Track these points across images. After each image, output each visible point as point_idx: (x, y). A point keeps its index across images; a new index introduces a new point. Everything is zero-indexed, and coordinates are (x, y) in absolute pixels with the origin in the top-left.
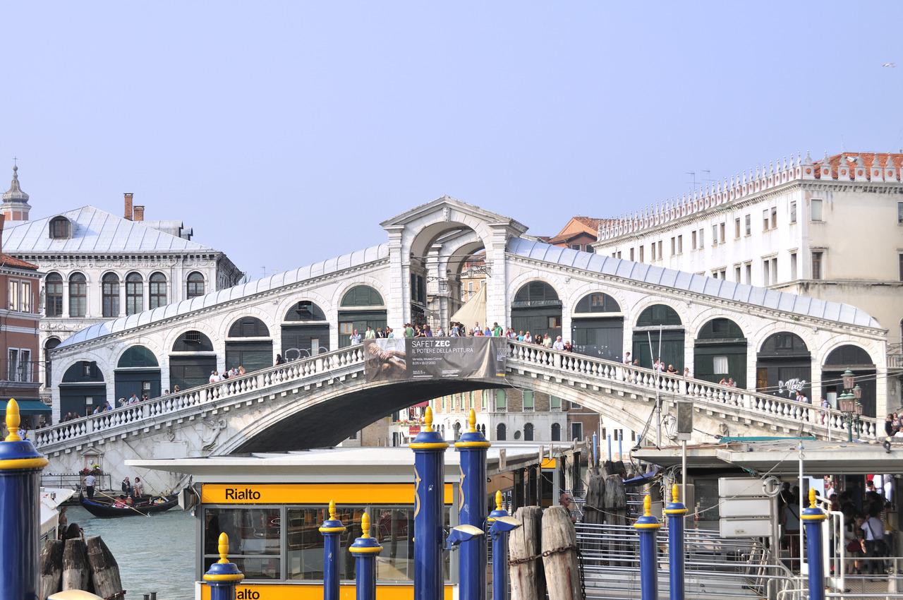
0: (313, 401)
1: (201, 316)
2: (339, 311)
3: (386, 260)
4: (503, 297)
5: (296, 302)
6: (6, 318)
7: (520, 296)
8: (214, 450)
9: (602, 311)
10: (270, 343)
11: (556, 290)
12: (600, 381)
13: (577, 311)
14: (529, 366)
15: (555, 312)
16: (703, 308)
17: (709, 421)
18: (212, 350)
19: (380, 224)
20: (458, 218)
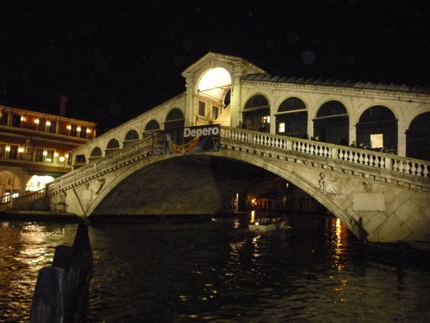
5: (149, 121)
7: (248, 105)
13: (279, 111)
16: (362, 100)
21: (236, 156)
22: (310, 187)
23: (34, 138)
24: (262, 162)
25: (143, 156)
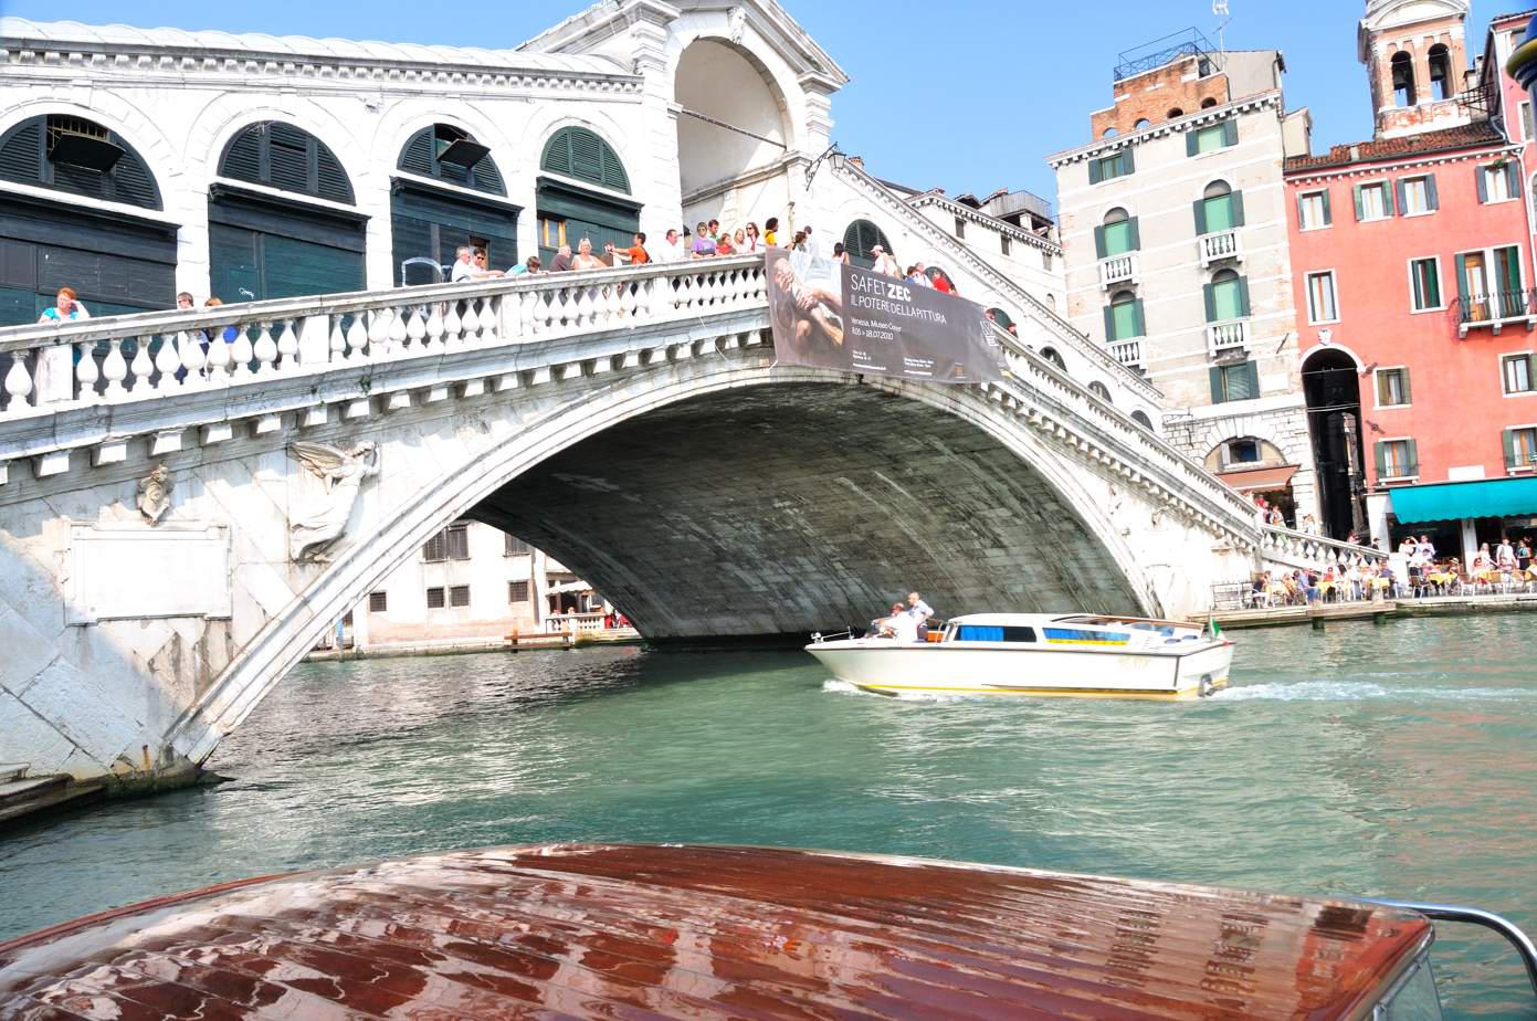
1: (114, 71)
2: (539, 180)
8: (338, 558)
10: (357, 224)
17: (1143, 506)
18: (155, 202)
20: (752, 42)
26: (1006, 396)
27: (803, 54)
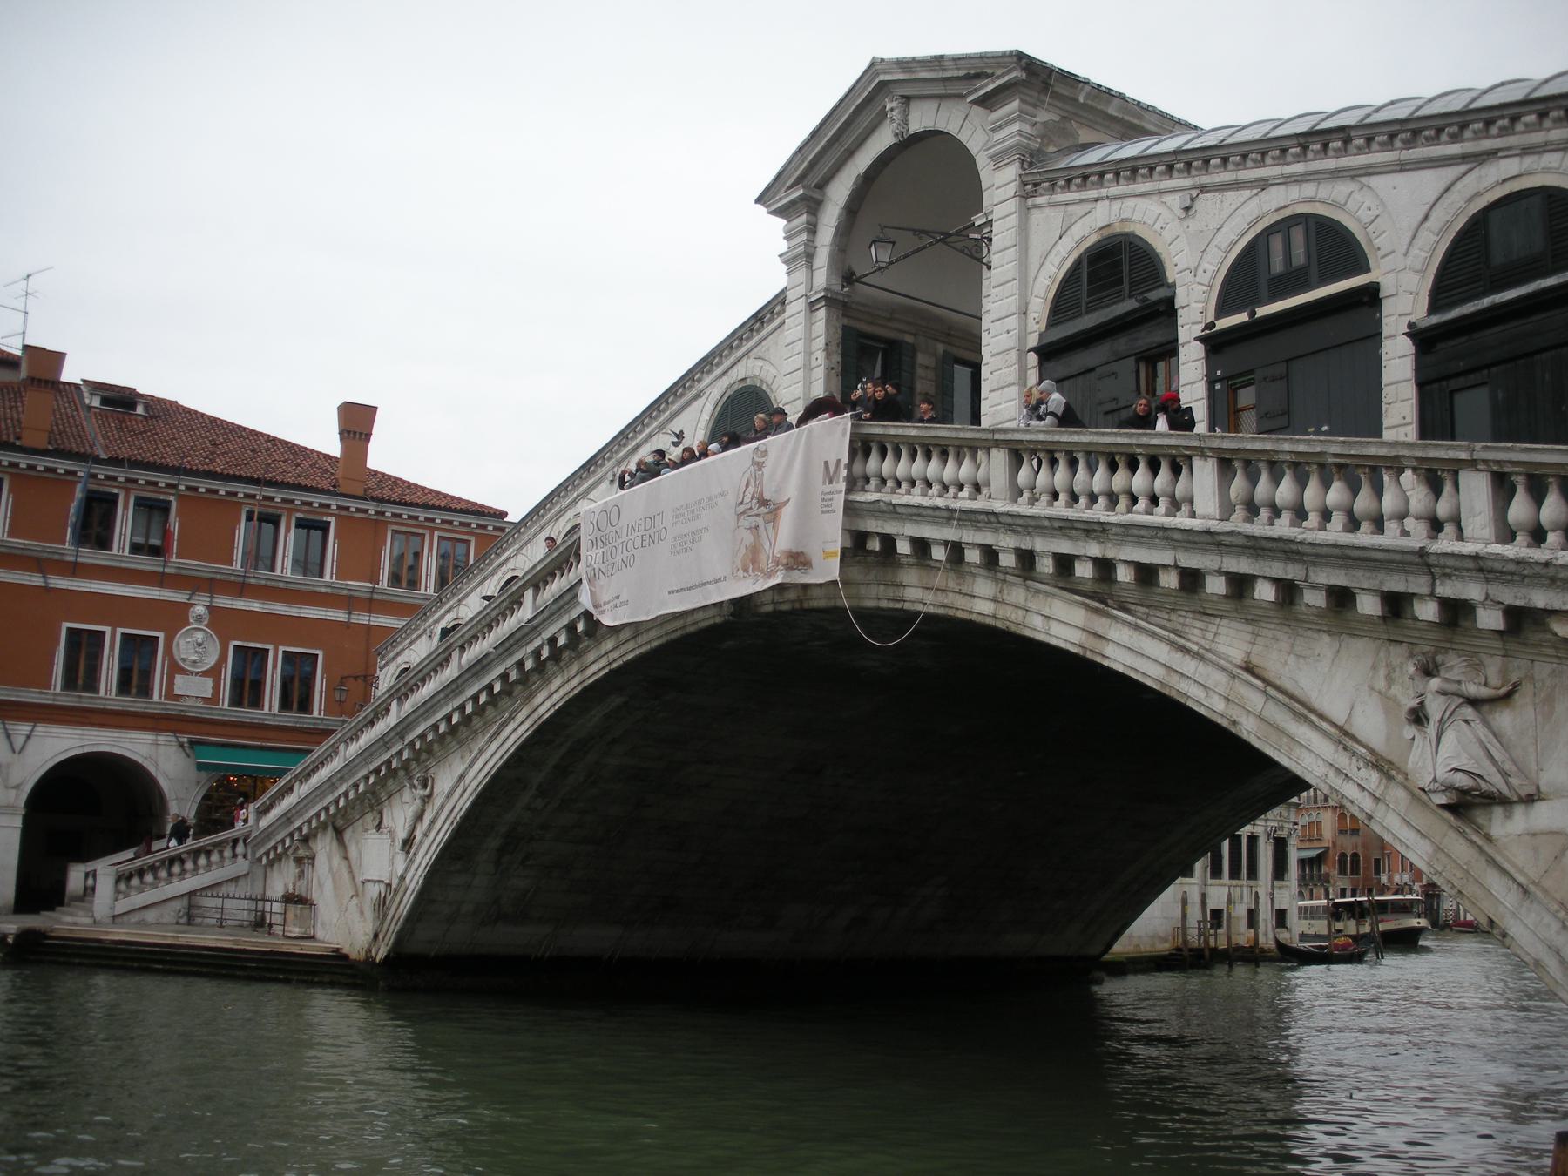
0: (536, 715)
3: (780, 301)
4: (1013, 322)
6: (371, 600)
9: (1305, 287)
11: (1159, 247)
12: (1130, 532)
13: (1223, 308)
14: (918, 514)
15: (1149, 337)
19: (758, 201)
20: (922, 119)
21: (949, 599)
22: (1343, 760)
23: (223, 602)
24: (1078, 615)
25: (552, 640)
26: (956, 551)
27: (958, 78)
